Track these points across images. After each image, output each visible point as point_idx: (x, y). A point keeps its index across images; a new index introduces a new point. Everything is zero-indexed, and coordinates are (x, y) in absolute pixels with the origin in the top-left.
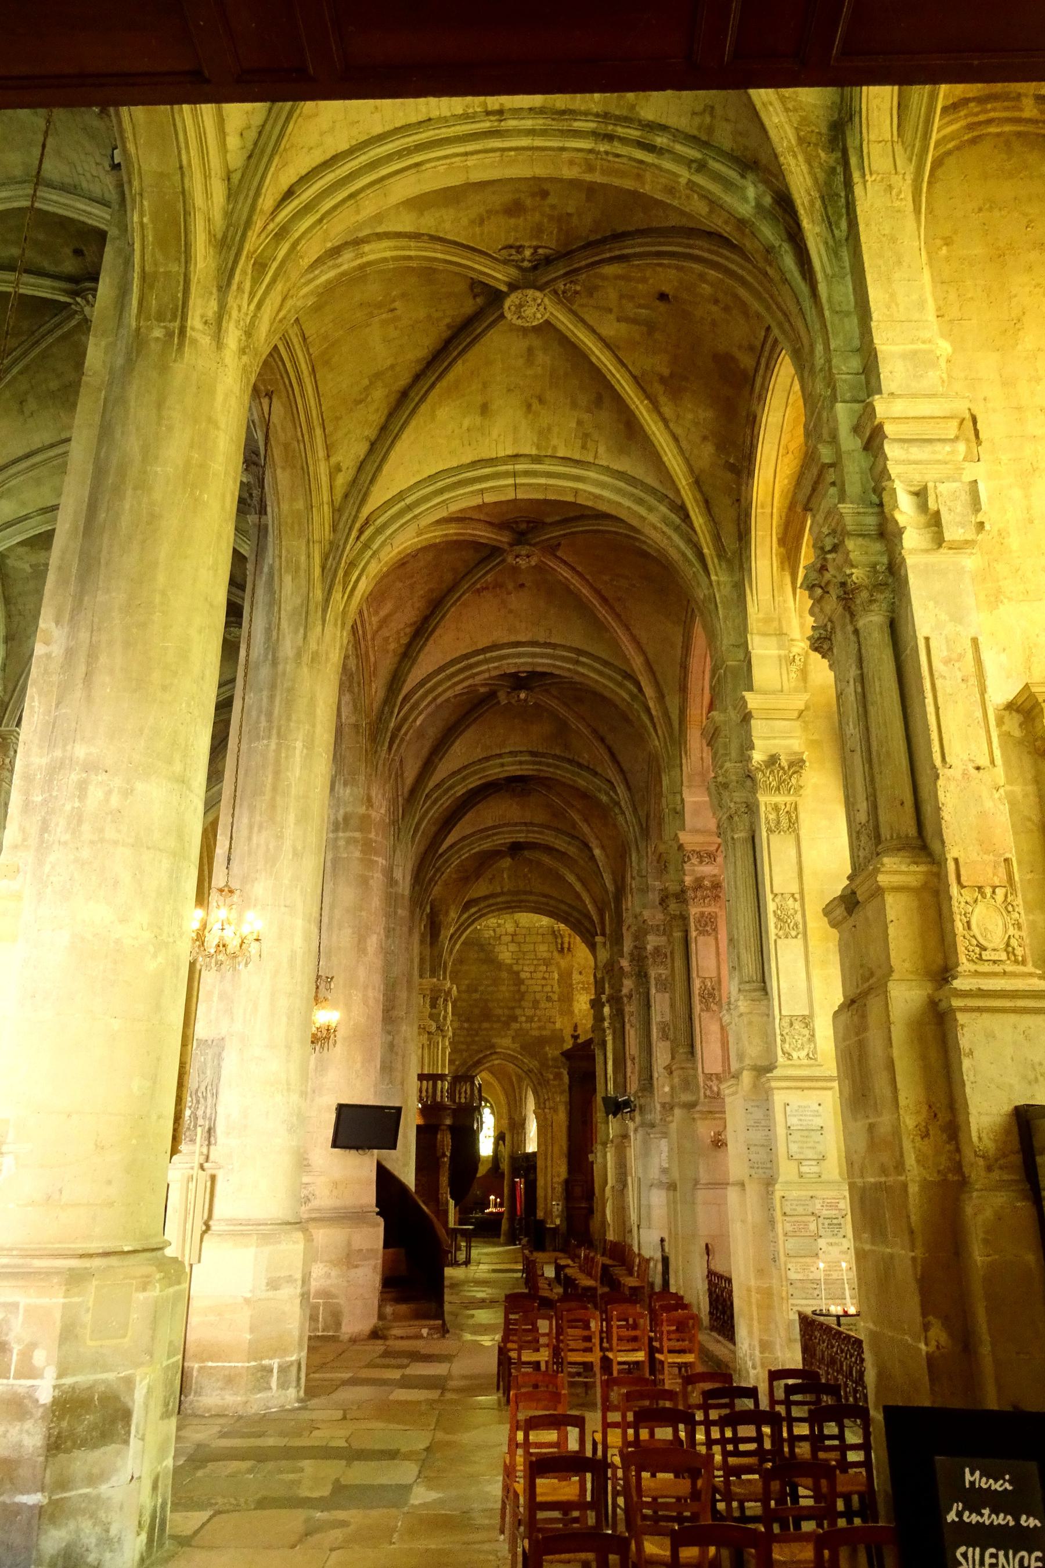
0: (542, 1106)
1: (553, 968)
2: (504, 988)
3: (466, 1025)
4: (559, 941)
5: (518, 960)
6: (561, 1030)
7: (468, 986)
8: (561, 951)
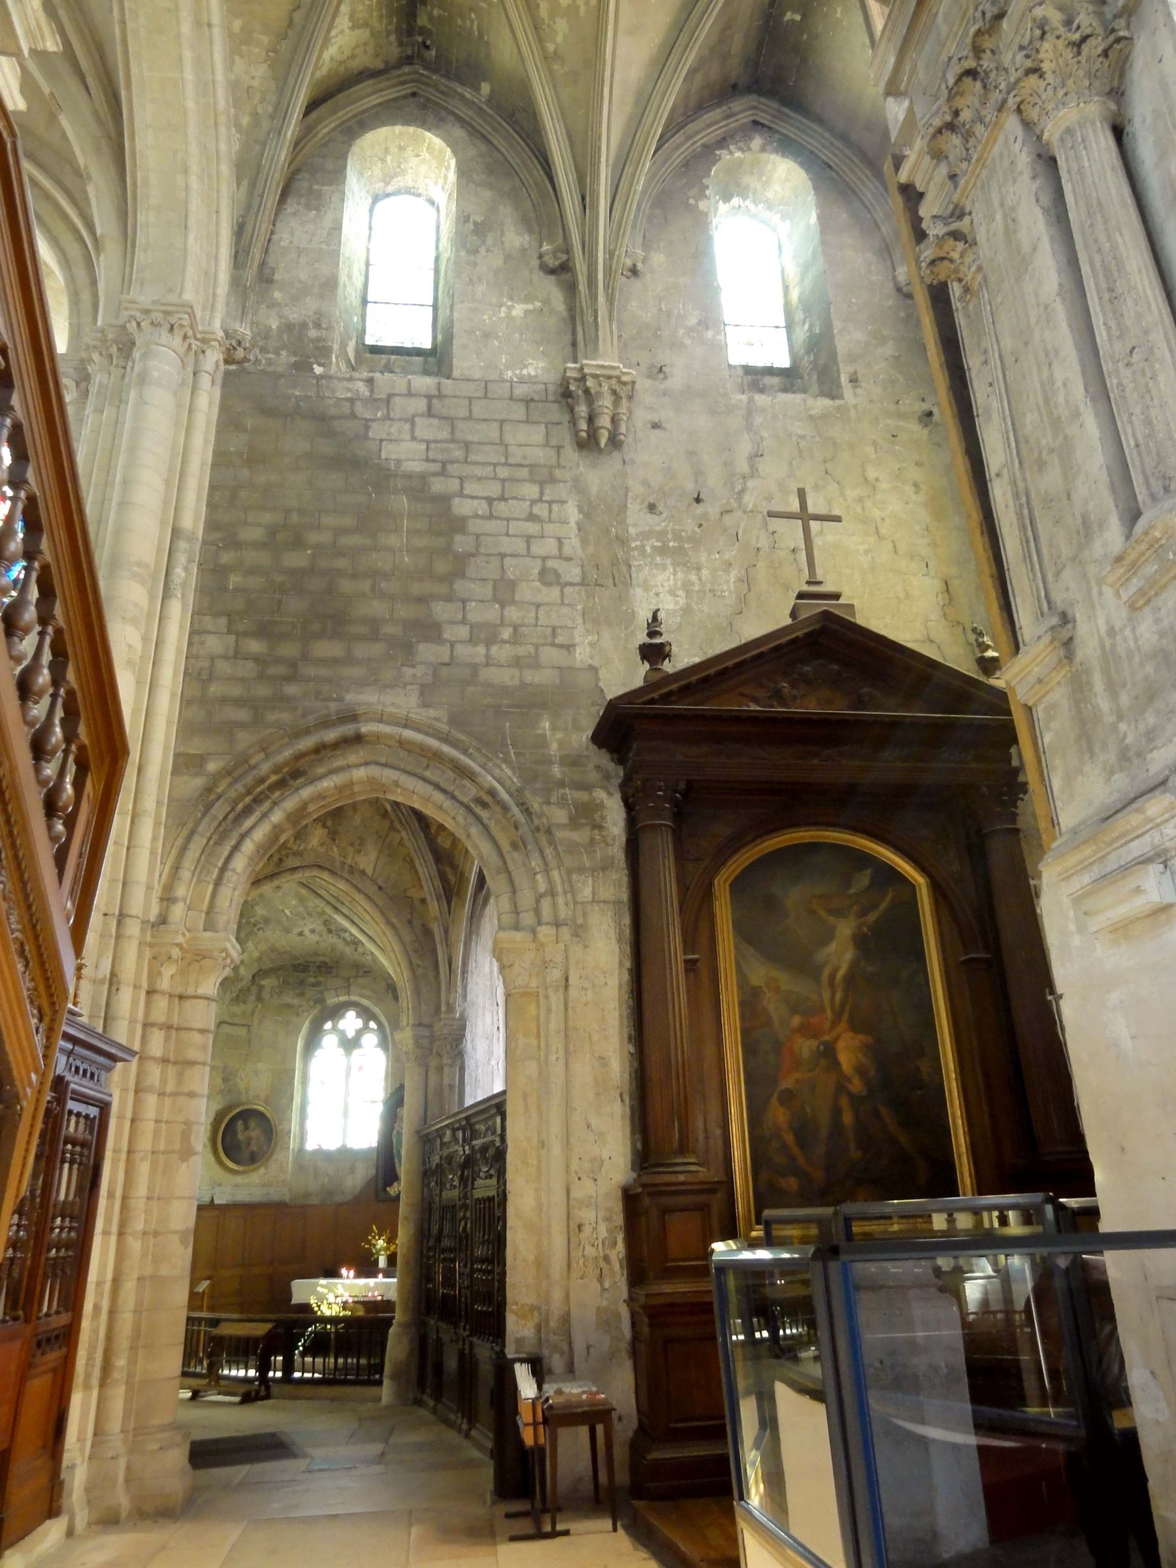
0: (528, 918)
1: (562, 490)
2: (393, 541)
3: (255, 646)
4: (582, 410)
5: (444, 464)
6: (594, 670)
7: (272, 531)
8: (588, 443)
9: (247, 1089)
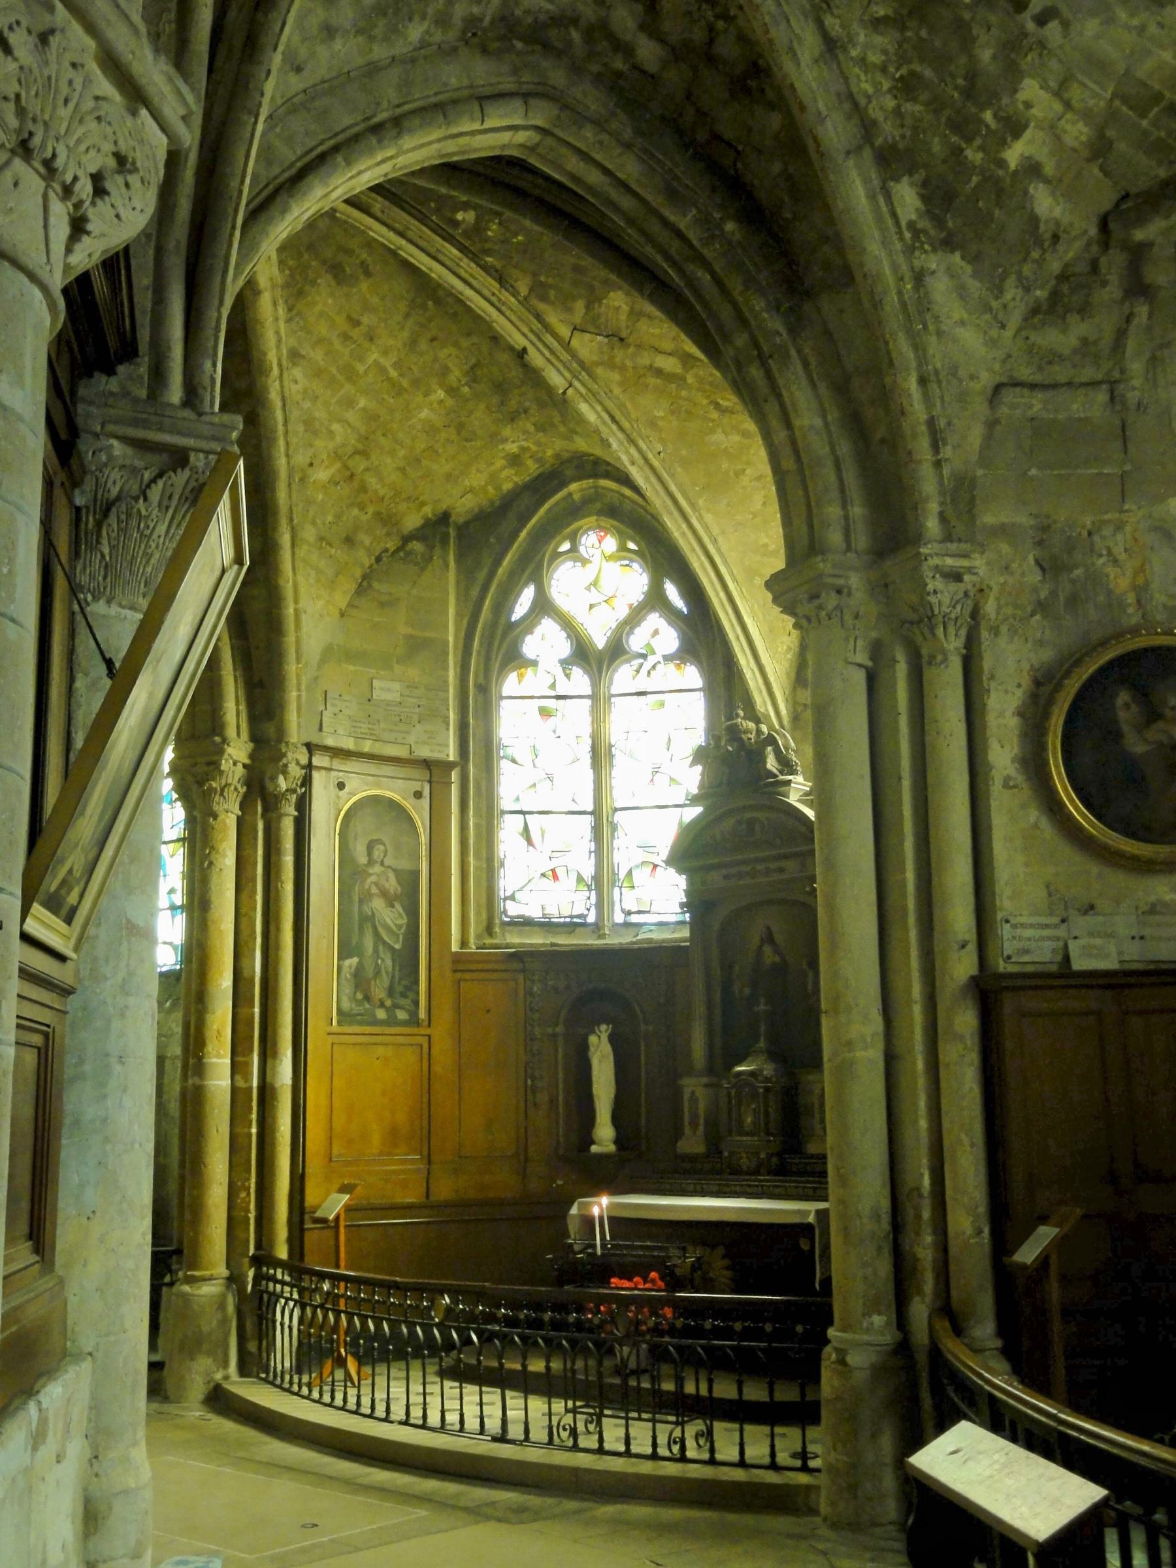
9: (1141, 591)
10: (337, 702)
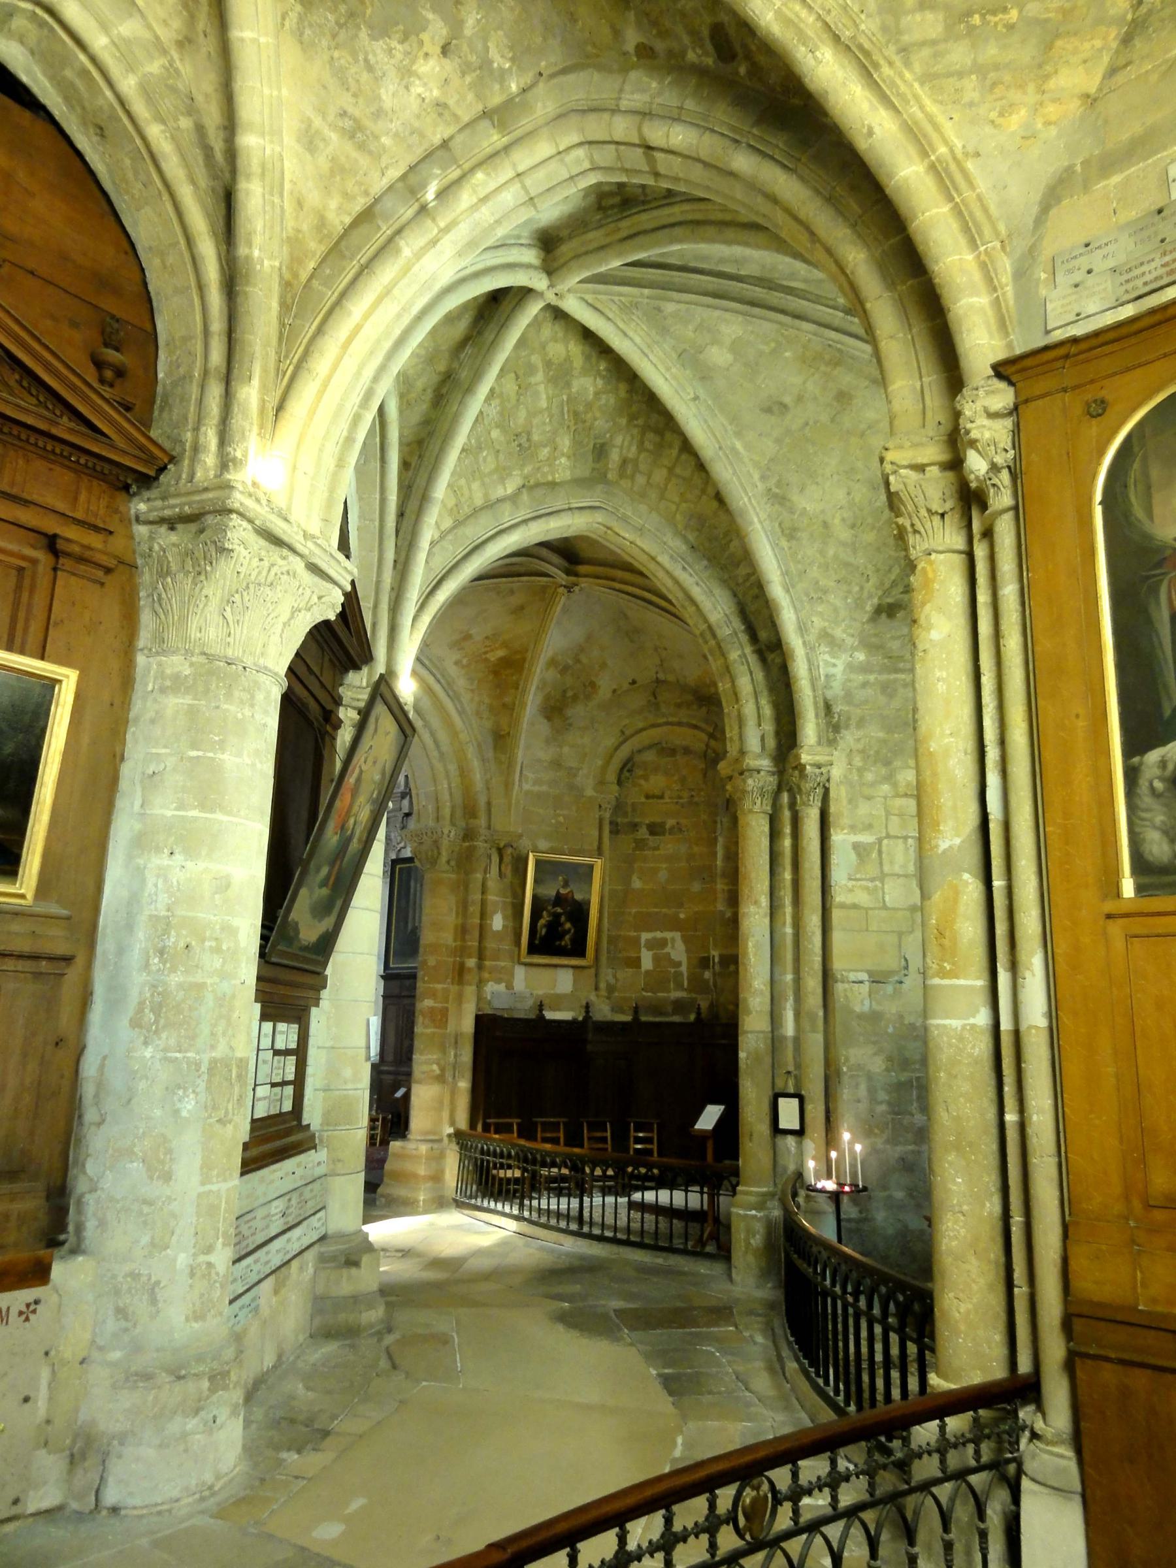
10: (1076, 263)
